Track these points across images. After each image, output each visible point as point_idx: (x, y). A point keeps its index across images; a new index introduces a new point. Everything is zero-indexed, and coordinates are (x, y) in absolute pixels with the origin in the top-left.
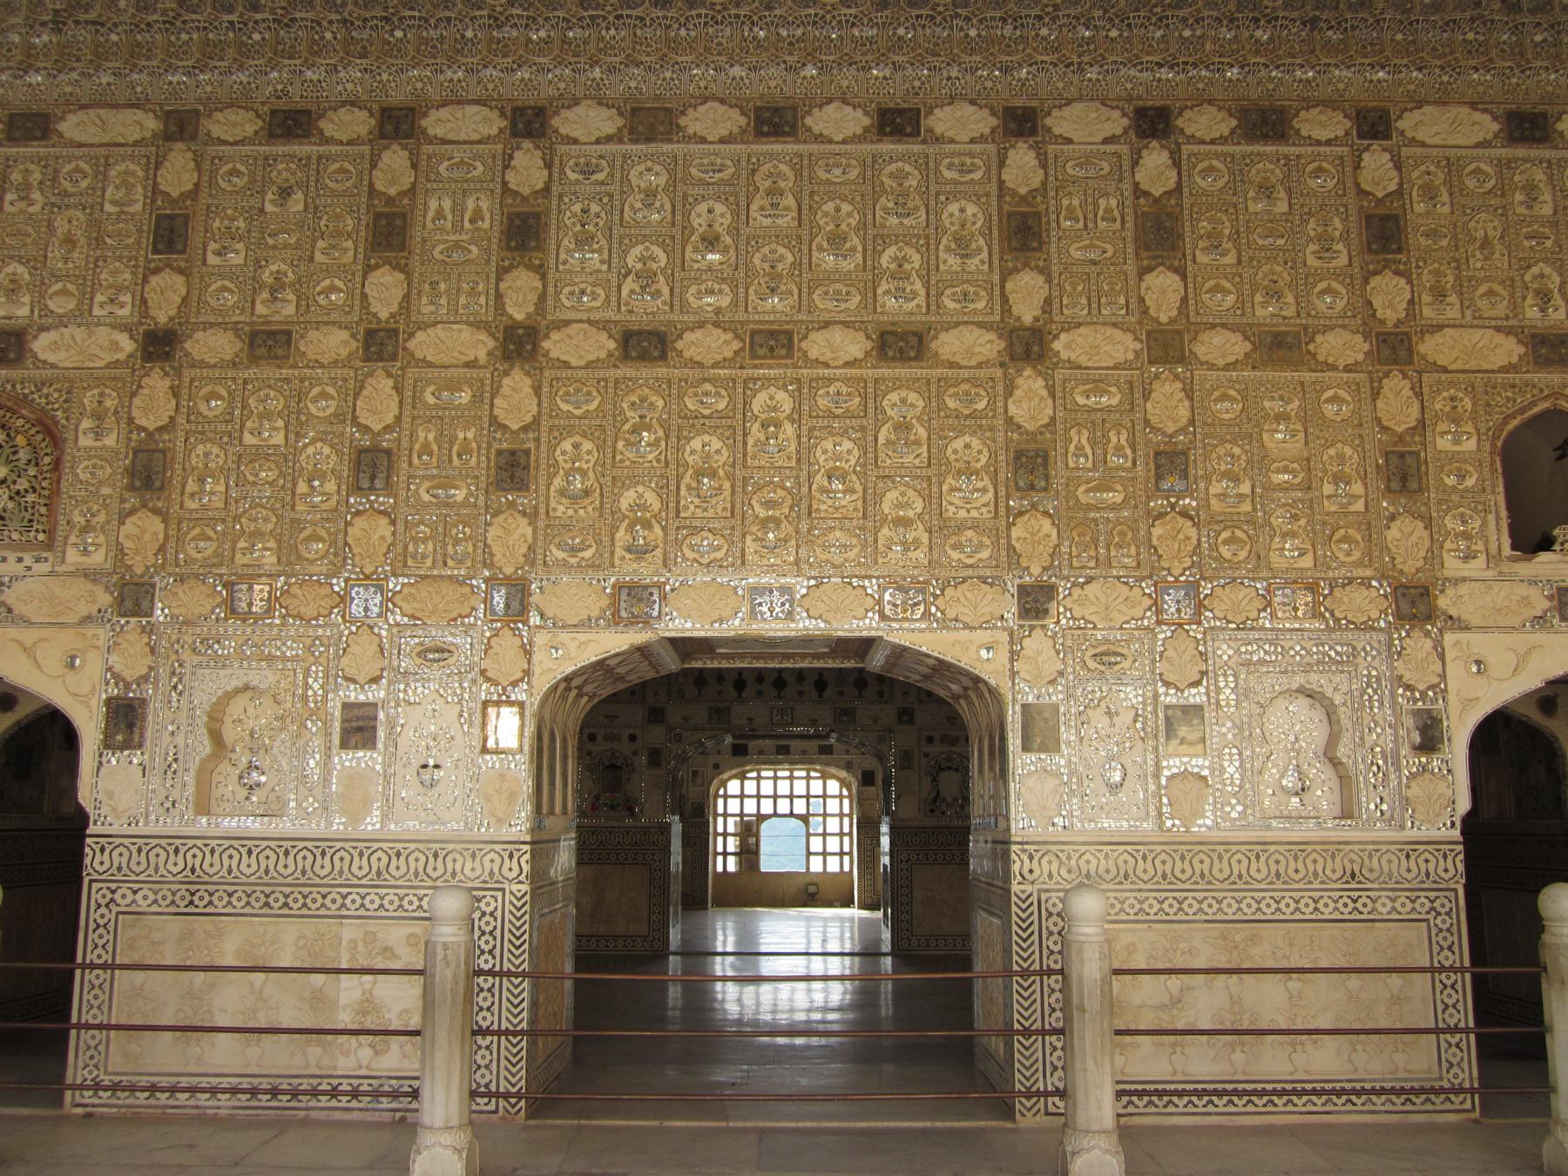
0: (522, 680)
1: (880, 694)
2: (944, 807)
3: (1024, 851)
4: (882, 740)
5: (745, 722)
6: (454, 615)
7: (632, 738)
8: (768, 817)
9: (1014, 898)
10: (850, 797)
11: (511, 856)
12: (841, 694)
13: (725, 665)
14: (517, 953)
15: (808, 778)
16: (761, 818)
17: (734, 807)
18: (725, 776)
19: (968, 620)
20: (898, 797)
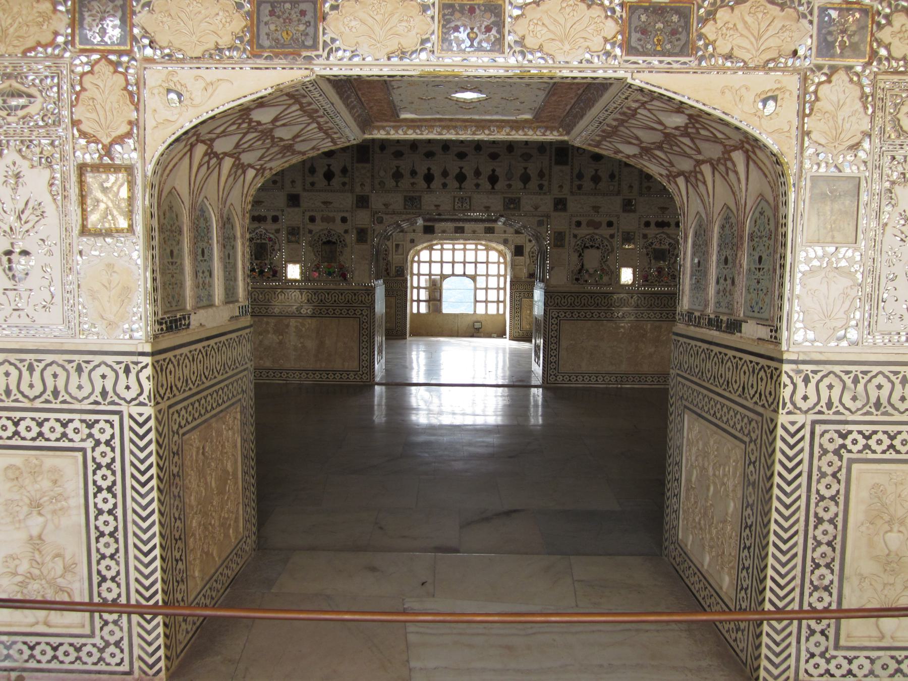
0: (129, 134)
1: (541, 187)
2: (586, 277)
3: (799, 372)
4: (540, 223)
5: (433, 208)
6: (30, 43)
7: (344, 220)
8: (449, 276)
9: (780, 432)
10: (505, 263)
11: (127, 371)
12: (509, 186)
13: (411, 135)
14: (143, 491)
15: (476, 250)
16: (443, 277)
17: (424, 269)
18: (419, 248)
19: (746, 56)
20: (552, 268)
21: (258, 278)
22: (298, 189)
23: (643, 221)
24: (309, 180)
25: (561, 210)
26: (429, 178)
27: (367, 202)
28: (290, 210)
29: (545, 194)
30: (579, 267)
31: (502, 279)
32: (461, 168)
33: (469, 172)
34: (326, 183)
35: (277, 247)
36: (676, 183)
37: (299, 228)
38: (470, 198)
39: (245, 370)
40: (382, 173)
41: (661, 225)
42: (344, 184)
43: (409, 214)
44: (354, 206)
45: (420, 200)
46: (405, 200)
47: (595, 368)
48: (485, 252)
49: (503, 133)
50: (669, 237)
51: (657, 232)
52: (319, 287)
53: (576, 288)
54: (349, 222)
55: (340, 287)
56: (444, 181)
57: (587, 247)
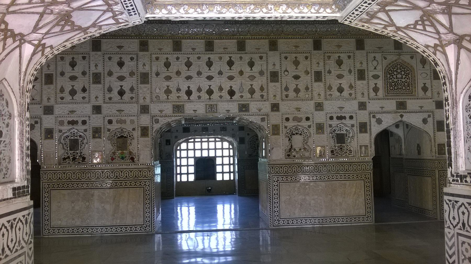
1: (262, 96)
4: (263, 120)
10: (233, 149)
12: (242, 97)
15: (215, 141)
21: (72, 163)
22: (100, 102)
23: (329, 116)
24: (108, 96)
25: (276, 111)
26: (189, 93)
27: (148, 109)
28: (94, 116)
29: (265, 101)
30: (289, 147)
31: (232, 158)
32: (210, 86)
33: (215, 88)
34: (120, 97)
35: (85, 141)
36: (445, 53)
37: (101, 128)
38: (216, 105)
39: (20, 256)
40: (158, 91)
41: (340, 118)
42: (132, 98)
43: (177, 116)
44: (139, 112)
45: (184, 107)
46: (173, 108)
47: (304, 214)
48: (221, 143)
49: (280, 11)
50: (346, 126)
51: (338, 123)
52: (114, 168)
53: (289, 161)
54: (136, 123)
55: (130, 167)
56: (198, 94)
57: (294, 134)
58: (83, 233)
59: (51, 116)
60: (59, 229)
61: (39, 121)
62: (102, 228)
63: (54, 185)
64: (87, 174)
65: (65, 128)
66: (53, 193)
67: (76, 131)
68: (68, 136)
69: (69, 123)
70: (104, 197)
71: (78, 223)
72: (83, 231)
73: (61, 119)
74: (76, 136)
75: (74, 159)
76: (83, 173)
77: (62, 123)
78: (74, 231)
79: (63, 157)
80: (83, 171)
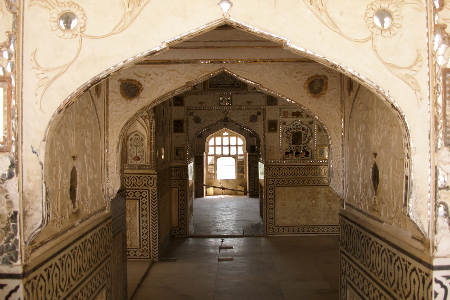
21: (295, 158)
35: (309, 134)
58: (308, 232)
59: (274, 107)
60: (284, 227)
61: (262, 112)
62: (328, 227)
63: (278, 181)
64: (313, 170)
65: (290, 120)
66: (278, 189)
67: (299, 123)
68: (291, 129)
69: (293, 114)
70: (331, 195)
71: (303, 221)
72: (308, 231)
73: (285, 110)
74: (299, 129)
75: (297, 153)
76: (309, 169)
77: (286, 114)
78: (299, 230)
79: (286, 151)
80: (309, 167)
